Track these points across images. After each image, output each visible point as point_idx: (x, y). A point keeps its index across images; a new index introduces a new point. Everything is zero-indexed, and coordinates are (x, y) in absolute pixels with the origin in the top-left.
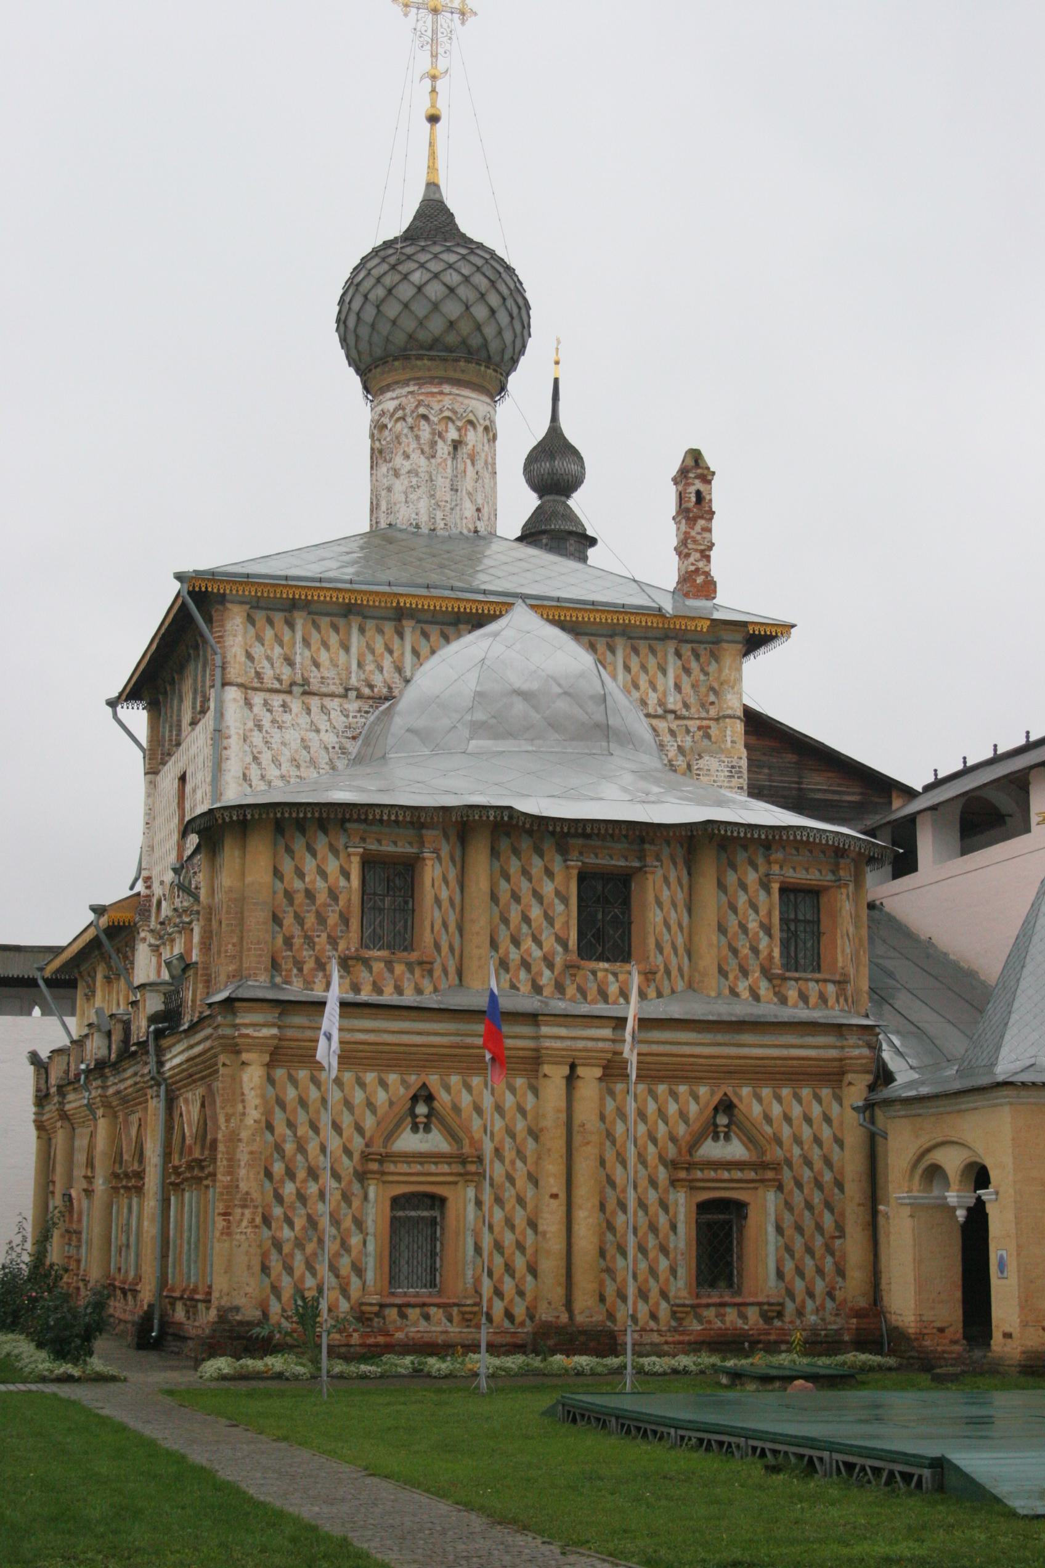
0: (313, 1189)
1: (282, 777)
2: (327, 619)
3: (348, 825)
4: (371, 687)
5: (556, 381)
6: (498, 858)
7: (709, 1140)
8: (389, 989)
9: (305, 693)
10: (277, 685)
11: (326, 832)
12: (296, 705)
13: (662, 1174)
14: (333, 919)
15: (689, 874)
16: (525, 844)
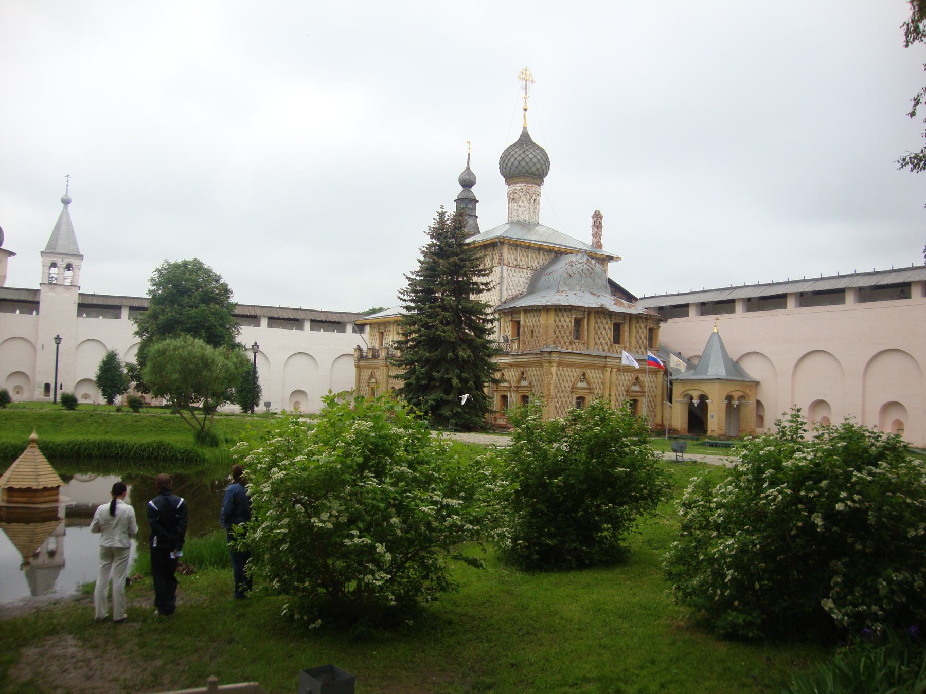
5: (469, 154)
8: (578, 349)
12: (517, 271)
13: (625, 393)
14: (568, 332)
16: (602, 316)
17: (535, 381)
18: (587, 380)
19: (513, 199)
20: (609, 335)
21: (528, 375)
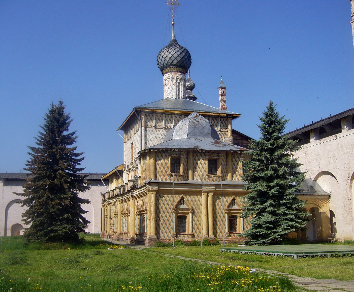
0: (164, 215)
1: (152, 143)
2: (159, 115)
3: (168, 152)
4: (167, 127)
6: (194, 157)
7: (231, 205)
10: (151, 127)
11: (164, 153)
12: (154, 130)
14: (166, 168)
15: (227, 159)
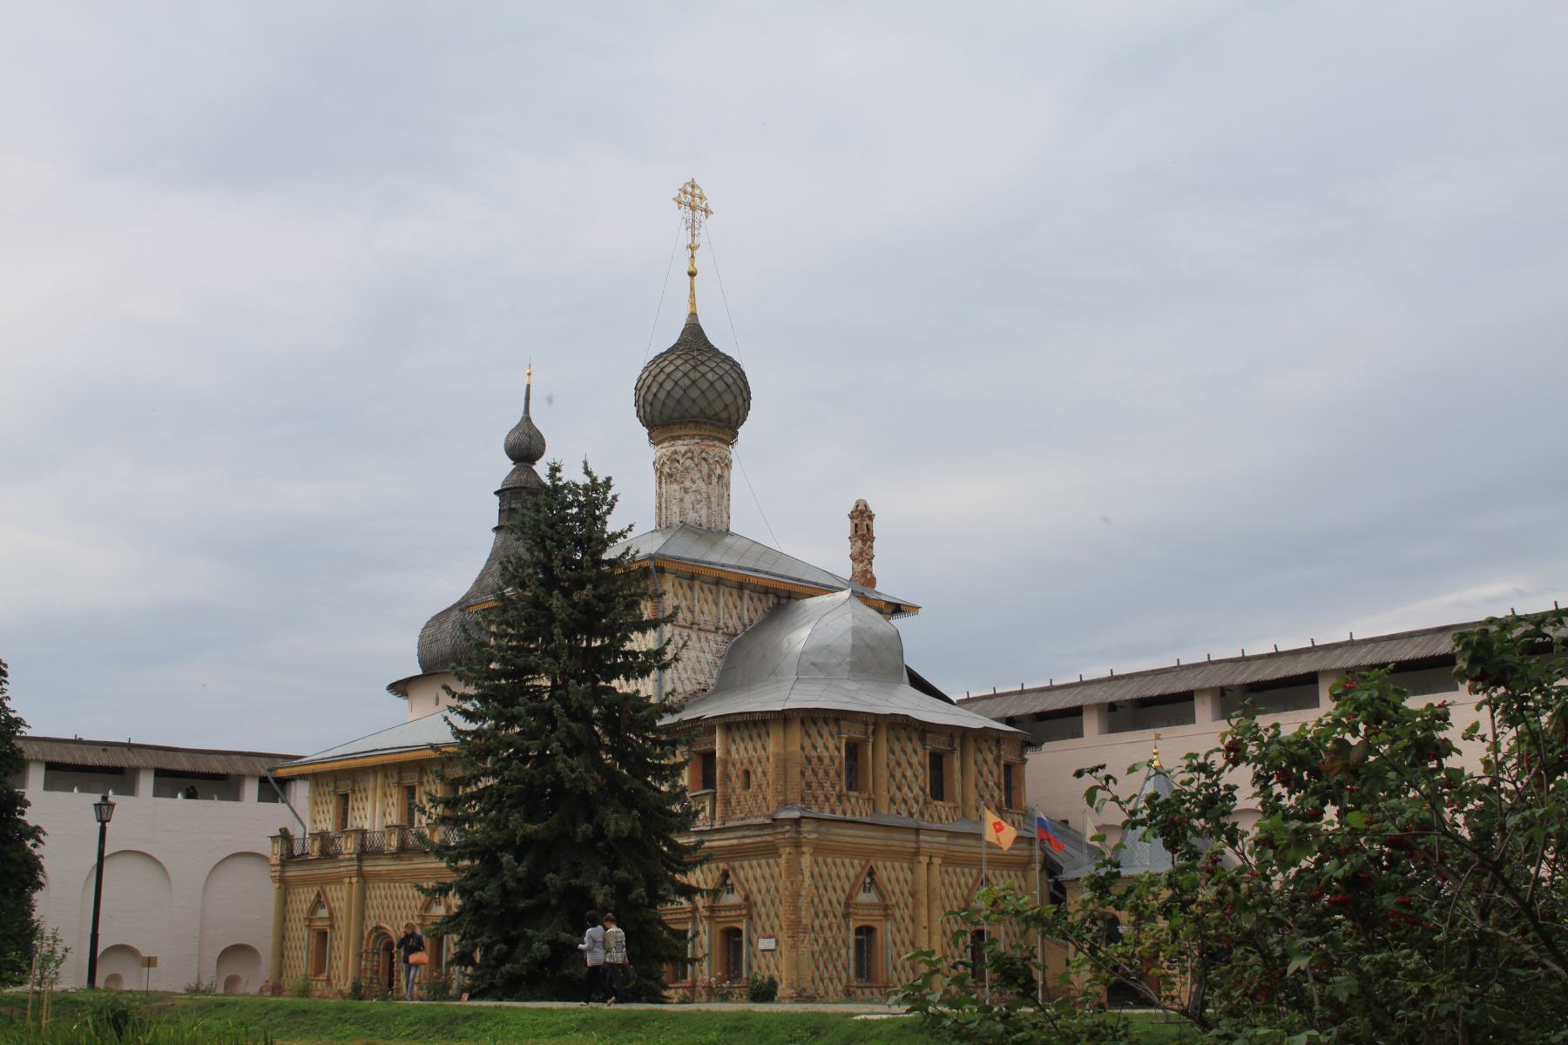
0: (826, 923)
1: (688, 679)
4: (727, 628)
5: (528, 386)
8: (857, 813)
9: (700, 629)
10: (684, 624)
11: (827, 724)
12: (694, 637)
14: (832, 773)
16: (903, 735)
17: (759, 891)
18: (878, 888)
19: (670, 475)
20: (920, 779)
21: (737, 877)
